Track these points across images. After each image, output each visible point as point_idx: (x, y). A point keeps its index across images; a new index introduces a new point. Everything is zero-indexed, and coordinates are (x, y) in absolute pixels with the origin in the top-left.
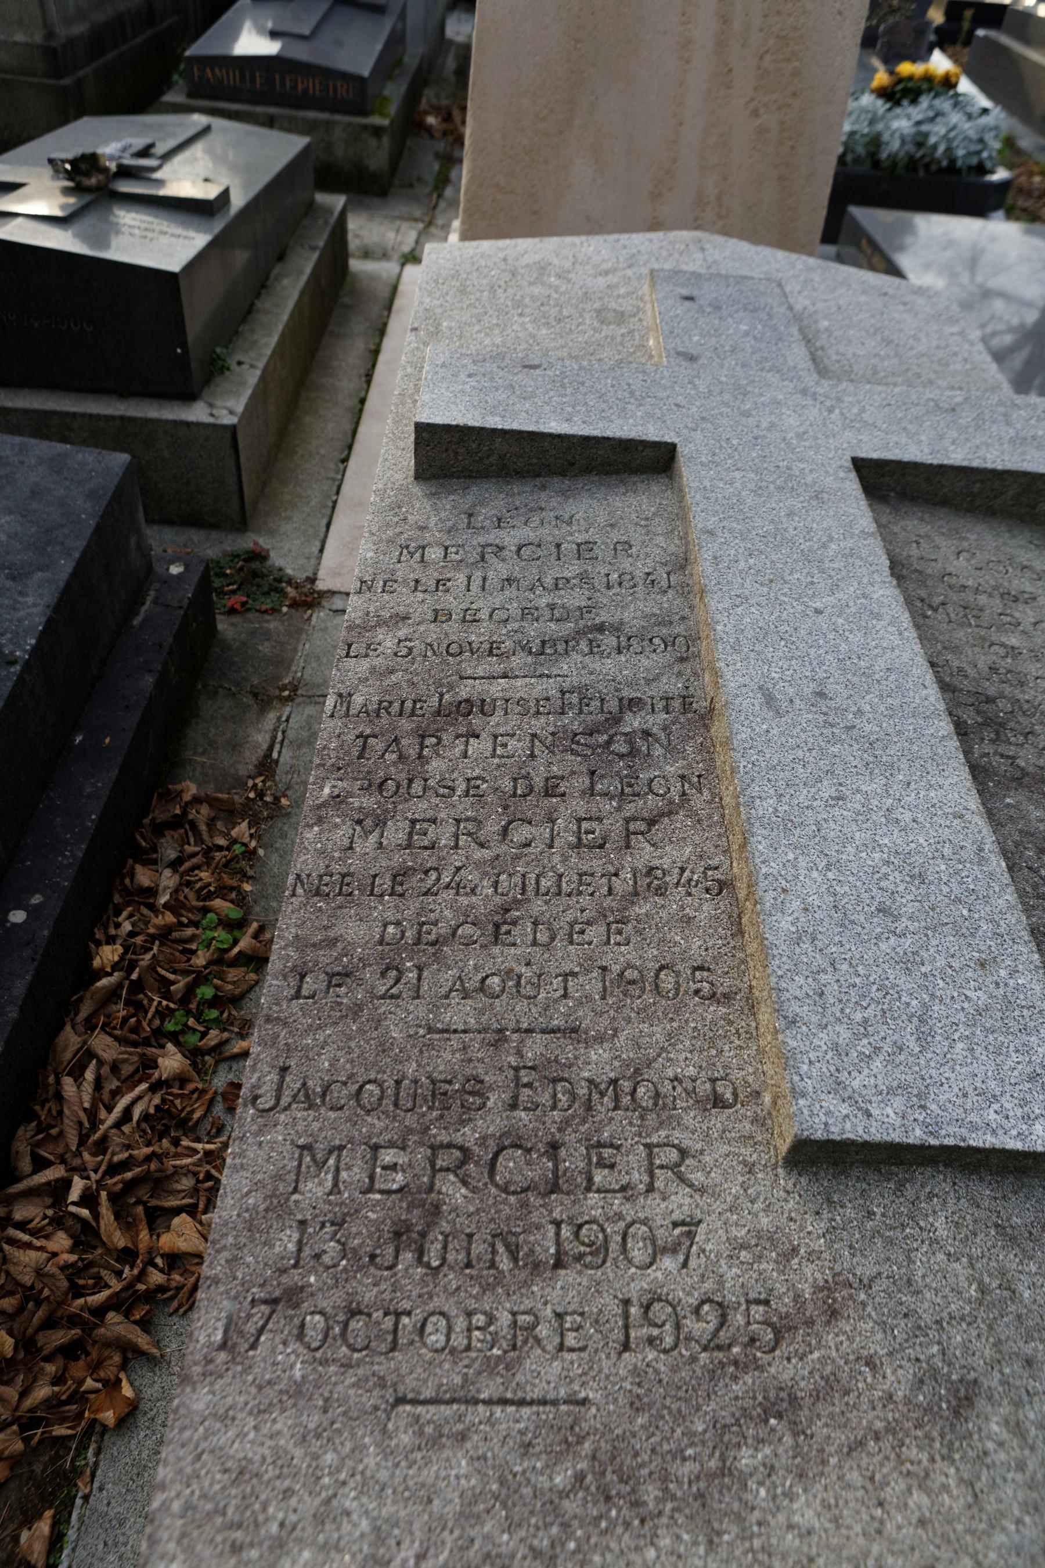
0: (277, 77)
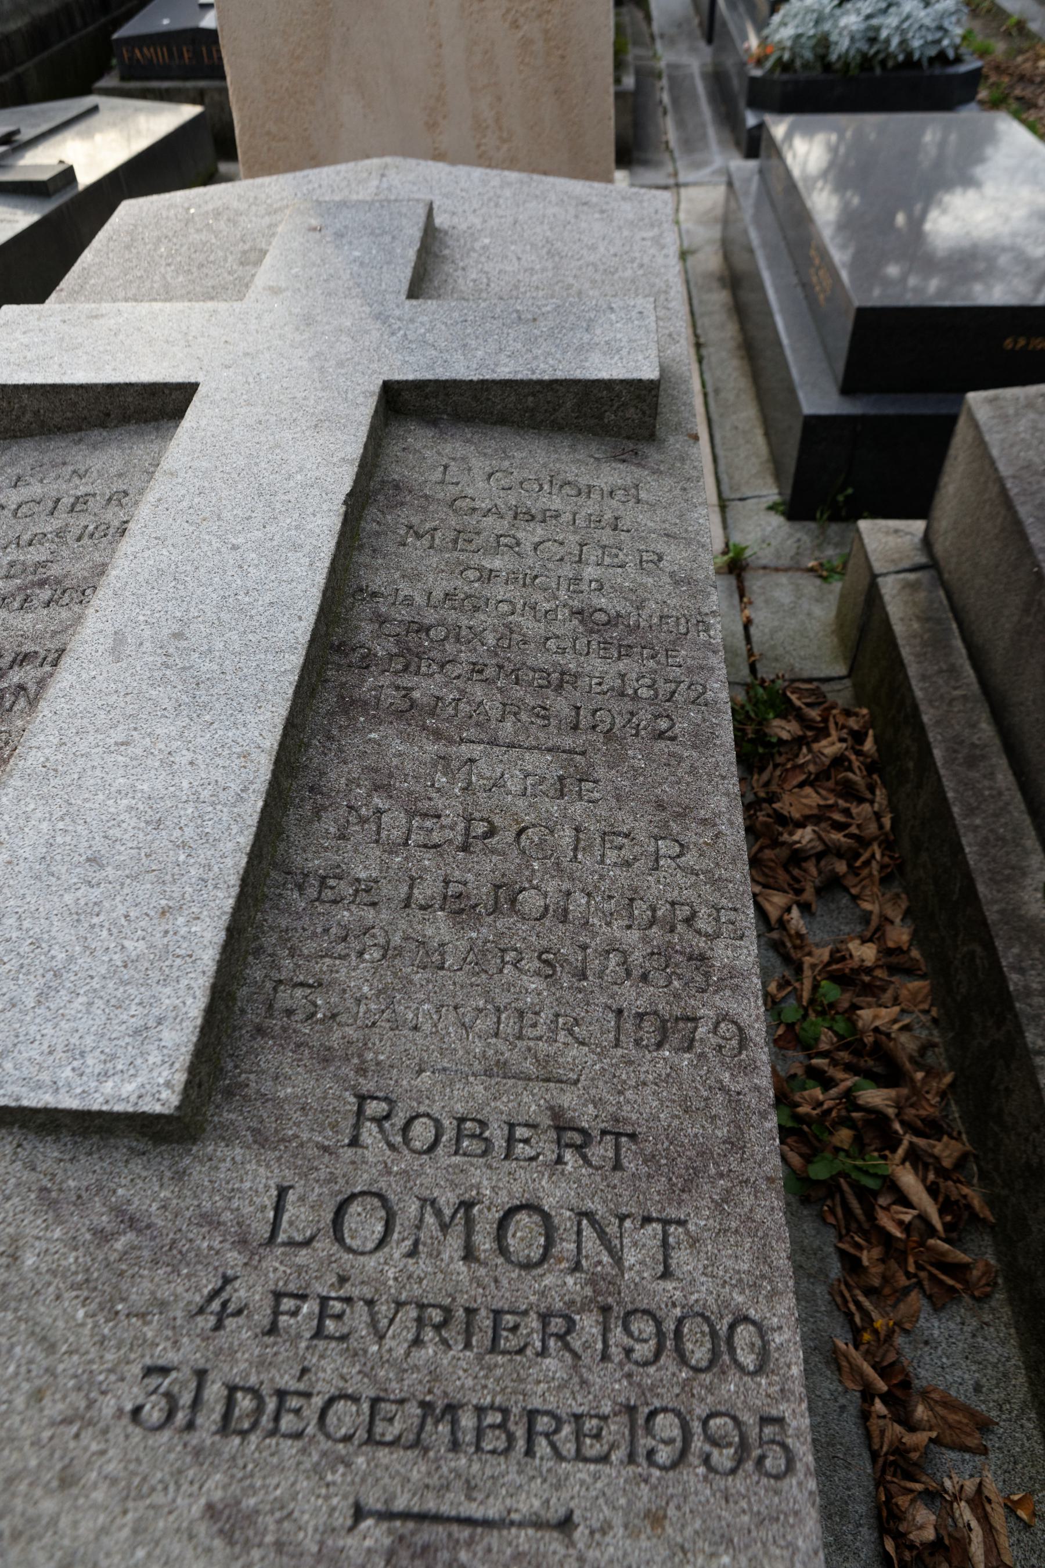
0: (204, 49)
